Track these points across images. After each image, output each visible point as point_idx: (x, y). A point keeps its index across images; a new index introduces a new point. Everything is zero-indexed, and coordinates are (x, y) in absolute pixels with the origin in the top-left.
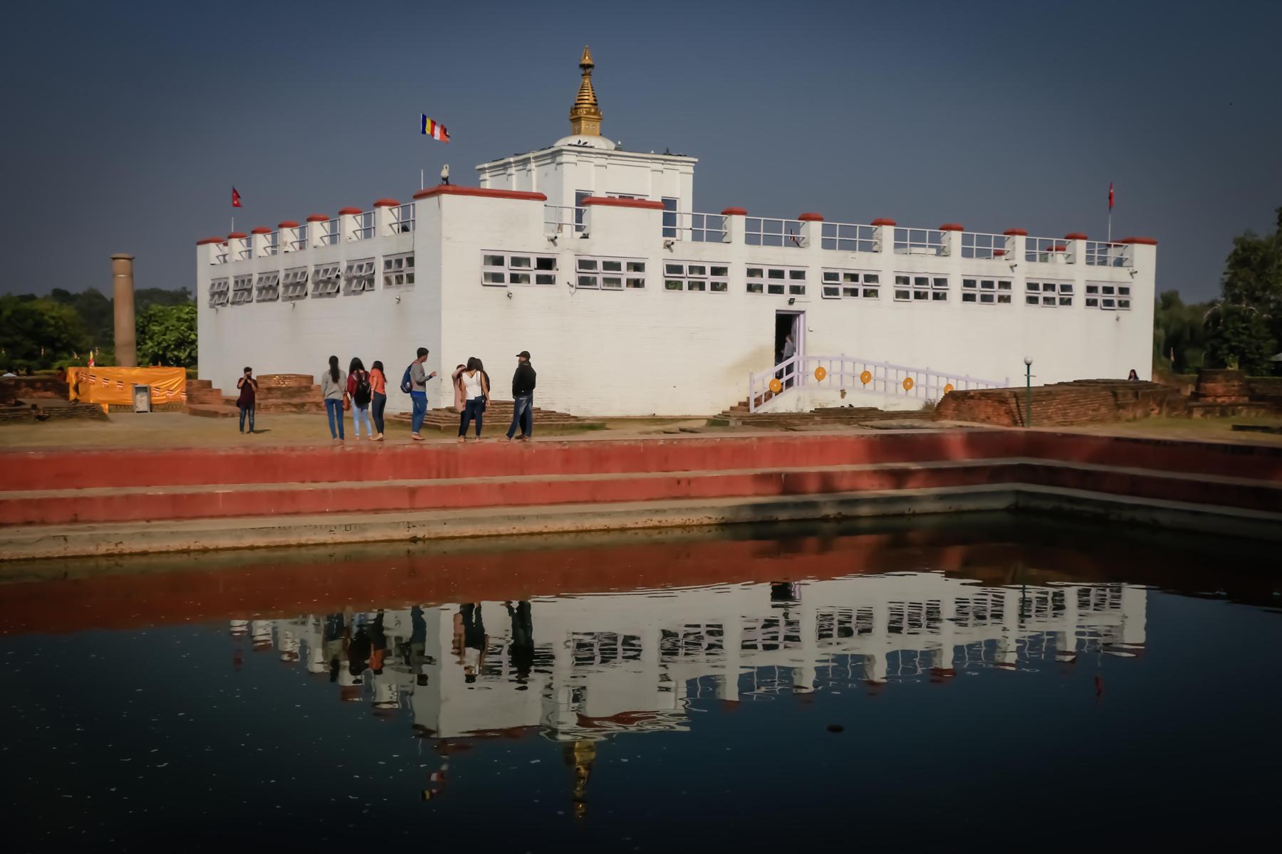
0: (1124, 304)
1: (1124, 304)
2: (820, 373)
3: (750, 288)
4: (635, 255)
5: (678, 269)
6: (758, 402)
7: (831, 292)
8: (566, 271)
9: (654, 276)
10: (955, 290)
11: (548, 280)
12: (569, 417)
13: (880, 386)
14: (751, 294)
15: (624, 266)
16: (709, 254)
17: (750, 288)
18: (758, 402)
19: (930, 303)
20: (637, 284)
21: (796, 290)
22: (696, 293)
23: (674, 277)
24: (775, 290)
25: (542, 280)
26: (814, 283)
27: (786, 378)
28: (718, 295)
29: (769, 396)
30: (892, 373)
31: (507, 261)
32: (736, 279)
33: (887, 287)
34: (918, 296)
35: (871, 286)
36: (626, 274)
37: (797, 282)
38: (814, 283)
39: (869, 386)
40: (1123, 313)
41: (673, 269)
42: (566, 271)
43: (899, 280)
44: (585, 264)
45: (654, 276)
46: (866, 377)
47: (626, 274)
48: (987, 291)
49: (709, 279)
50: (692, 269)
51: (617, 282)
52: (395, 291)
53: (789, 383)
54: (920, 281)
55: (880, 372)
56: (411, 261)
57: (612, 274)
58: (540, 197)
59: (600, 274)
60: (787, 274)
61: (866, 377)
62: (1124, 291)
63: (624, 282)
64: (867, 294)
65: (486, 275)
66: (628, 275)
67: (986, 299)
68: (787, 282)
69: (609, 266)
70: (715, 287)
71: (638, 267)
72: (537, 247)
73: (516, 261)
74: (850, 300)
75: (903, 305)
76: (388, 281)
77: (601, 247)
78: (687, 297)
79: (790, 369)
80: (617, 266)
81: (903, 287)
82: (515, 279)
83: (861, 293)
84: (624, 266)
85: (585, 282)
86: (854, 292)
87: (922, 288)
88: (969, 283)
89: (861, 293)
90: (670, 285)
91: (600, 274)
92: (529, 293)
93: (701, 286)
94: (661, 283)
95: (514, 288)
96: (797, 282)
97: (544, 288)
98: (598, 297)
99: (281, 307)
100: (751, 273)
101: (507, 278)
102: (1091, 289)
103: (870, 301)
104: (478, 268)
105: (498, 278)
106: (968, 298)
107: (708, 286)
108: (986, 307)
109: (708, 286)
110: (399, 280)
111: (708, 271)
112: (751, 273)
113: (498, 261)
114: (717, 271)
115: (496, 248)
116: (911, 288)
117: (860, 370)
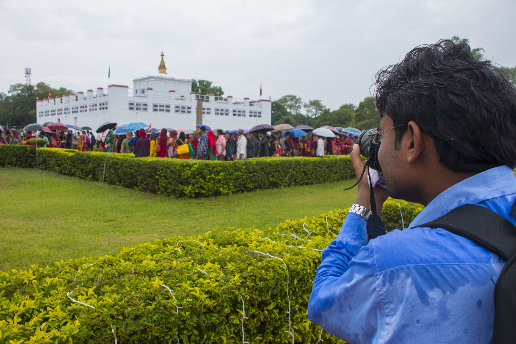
3: (177, 111)
5: (157, 106)
20: (146, 109)
22: (161, 112)
28: (168, 113)
34: (222, 114)
35: (208, 111)
37: (189, 110)
49: (165, 108)
50: (160, 106)
54: (222, 110)
59: (135, 107)
68: (186, 110)
81: (217, 112)
87: (222, 112)
90: (155, 110)
93: (163, 110)
100: (177, 107)
107: (165, 110)
109: (165, 110)
111: (165, 106)
116: (219, 112)
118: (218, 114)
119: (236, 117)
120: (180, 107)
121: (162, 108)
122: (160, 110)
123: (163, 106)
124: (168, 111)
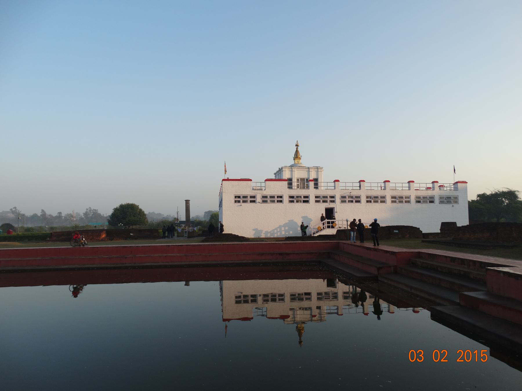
0: (456, 202)
1: (456, 202)
3: (317, 201)
4: (280, 194)
6: (314, 234)
8: (259, 199)
9: (286, 199)
12: (243, 237)
14: (317, 204)
15: (276, 197)
16: (303, 192)
18: (314, 234)
20: (281, 201)
21: (333, 201)
23: (292, 199)
24: (324, 202)
25: (251, 202)
26: (338, 199)
29: (317, 232)
32: (312, 199)
36: (276, 199)
40: (455, 205)
45: (286, 199)
47: (276, 199)
51: (274, 201)
57: (273, 199)
58: (251, 180)
59: (269, 200)
60: (328, 197)
63: (276, 201)
65: (235, 202)
66: (280, 199)
69: (271, 197)
71: (281, 197)
72: (248, 192)
73: (244, 197)
74: (351, 204)
75: (369, 204)
77: (268, 192)
80: (273, 197)
82: (244, 202)
83: (354, 201)
84: (276, 197)
85: (264, 202)
89: (354, 201)
91: (269, 200)
94: (288, 201)
95: (244, 205)
97: (253, 204)
101: (241, 201)
104: (233, 200)
105: (239, 202)
111: (302, 197)
112: (316, 197)
113: (239, 197)
114: (305, 197)
115: (238, 194)
121: (299, 199)
122: (297, 202)
123: (301, 197)
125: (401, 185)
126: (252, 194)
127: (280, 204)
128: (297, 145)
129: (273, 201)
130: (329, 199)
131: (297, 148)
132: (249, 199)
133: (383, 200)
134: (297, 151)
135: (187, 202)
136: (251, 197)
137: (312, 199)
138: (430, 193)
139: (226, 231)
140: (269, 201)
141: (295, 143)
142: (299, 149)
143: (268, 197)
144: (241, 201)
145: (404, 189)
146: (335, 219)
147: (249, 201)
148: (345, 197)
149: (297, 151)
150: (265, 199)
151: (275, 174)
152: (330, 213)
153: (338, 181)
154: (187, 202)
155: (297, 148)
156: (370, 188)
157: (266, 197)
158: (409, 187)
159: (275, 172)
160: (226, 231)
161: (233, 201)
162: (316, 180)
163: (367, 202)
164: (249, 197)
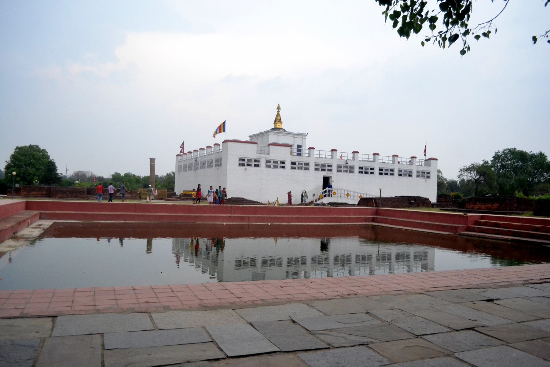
0: (428, 177)
1: (428, 177)
2: (335, 193)
3: (316, 169)
4: (282, 159)
6: (316, 201)
7: (339, 171)
9: (288, 165)
10: (377, 171)
11: (258, 166)
13: (352, 198)
15: (279, 163)
17: (316, 169)
18: (316, 201)
19: (369, 175)
20: (283, 167)
22: (300, 171)
24: (323, 170)
25: (255, 165)
26: (335, 168)
27: (324, 194)
29: (319, 199)
30: (343, 192)
31: (246, 160)
32: (312, 167)
33: (356, 170)
34: (366, 173)
35: (351, 170)
36: (279, 165)
37: (330, 168)
38: (335, 168)
39: (349, 197)
40: (428, 179)
41: (293, 163)
42: (263, 164)
43: (360, 168)
44: (267, 162)
45: (288, 165)
46: (348, 195)
47: (279, 165)
48: (387, 172)
49: (304, 166)
50: (299, 164)
51: (276, 167)
52: (217, 168)
53: (325, 196)
55: (352, 194)
56: (221, 159)
57: (276, 164)
58: (256, 143)
59: (272, 164)
61: (348, 195)
62: (428, 173)
64: (351, 172)
67: (387, 174)
68: (327, 168)
69: (274, 162)
70: (306, 169)
71: (283, 163)
73: (248, 160)
75: (361, 174)
76: (216, 166)
78: (297, 171)
79: (325, 192)
82: (248, 165)
85: (268, 166)
86: (346, 171)
88: (381, 170)
91: (272, 164)
92: (252, 169)
93: (302, 169)
94: (290, 168)
95: (248, 168)
96: (330, 168)
97: (256, 168)
98: (271, 170)
99: (193, 172)
101: (246, 165)
102: (418, 172)
103: (351, 174)
104: (237, 162)
105: (243, 165)
106: (381, 174)
108: (386, 176)
110: (218, 166)
112: (316, 165)
113: (243, 160)
115: (243, 157)
117: (346, 193)
118: (362, 172)
119: (384, 176)
120: (320, 165)
122: (298, 168)
123: (302, 164)
124: (307, 169)
125: (346, 155)
126: (257, 158)
127: (282, 170)
128: (279, 109)
129: (276, 167)
130: (327, 168)
131: (278, 112)
132: (253, 163)
133: (351, 170)
134: (278, 115)
135: (152, 161)
136: (255, 161)
137: (312, 167)
138: (409, 168)
139: (229, 196)
140: (272, 166)
141: (277, 106)
142: (280, 113)
143: (272, 162)
144: (246, 165)
145: (327, 157)
146: (331, 187)
147: (253, 165)
148: (341, 167)
149: (278, 115)
150: (268, 164)
151: (250, 137)
152: (326, 182)
153: (336, 150)
154: (152, 161)
155: (278, 112)
156: (318, 156)
157: (270, 162)
158: (332, 156)
159: (251, 134)
160: (229, 196)
161: (238, 164)
162: (299, 147)
163: (359, 172)
164: (253, 161)
